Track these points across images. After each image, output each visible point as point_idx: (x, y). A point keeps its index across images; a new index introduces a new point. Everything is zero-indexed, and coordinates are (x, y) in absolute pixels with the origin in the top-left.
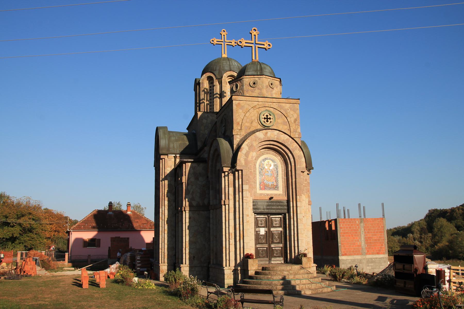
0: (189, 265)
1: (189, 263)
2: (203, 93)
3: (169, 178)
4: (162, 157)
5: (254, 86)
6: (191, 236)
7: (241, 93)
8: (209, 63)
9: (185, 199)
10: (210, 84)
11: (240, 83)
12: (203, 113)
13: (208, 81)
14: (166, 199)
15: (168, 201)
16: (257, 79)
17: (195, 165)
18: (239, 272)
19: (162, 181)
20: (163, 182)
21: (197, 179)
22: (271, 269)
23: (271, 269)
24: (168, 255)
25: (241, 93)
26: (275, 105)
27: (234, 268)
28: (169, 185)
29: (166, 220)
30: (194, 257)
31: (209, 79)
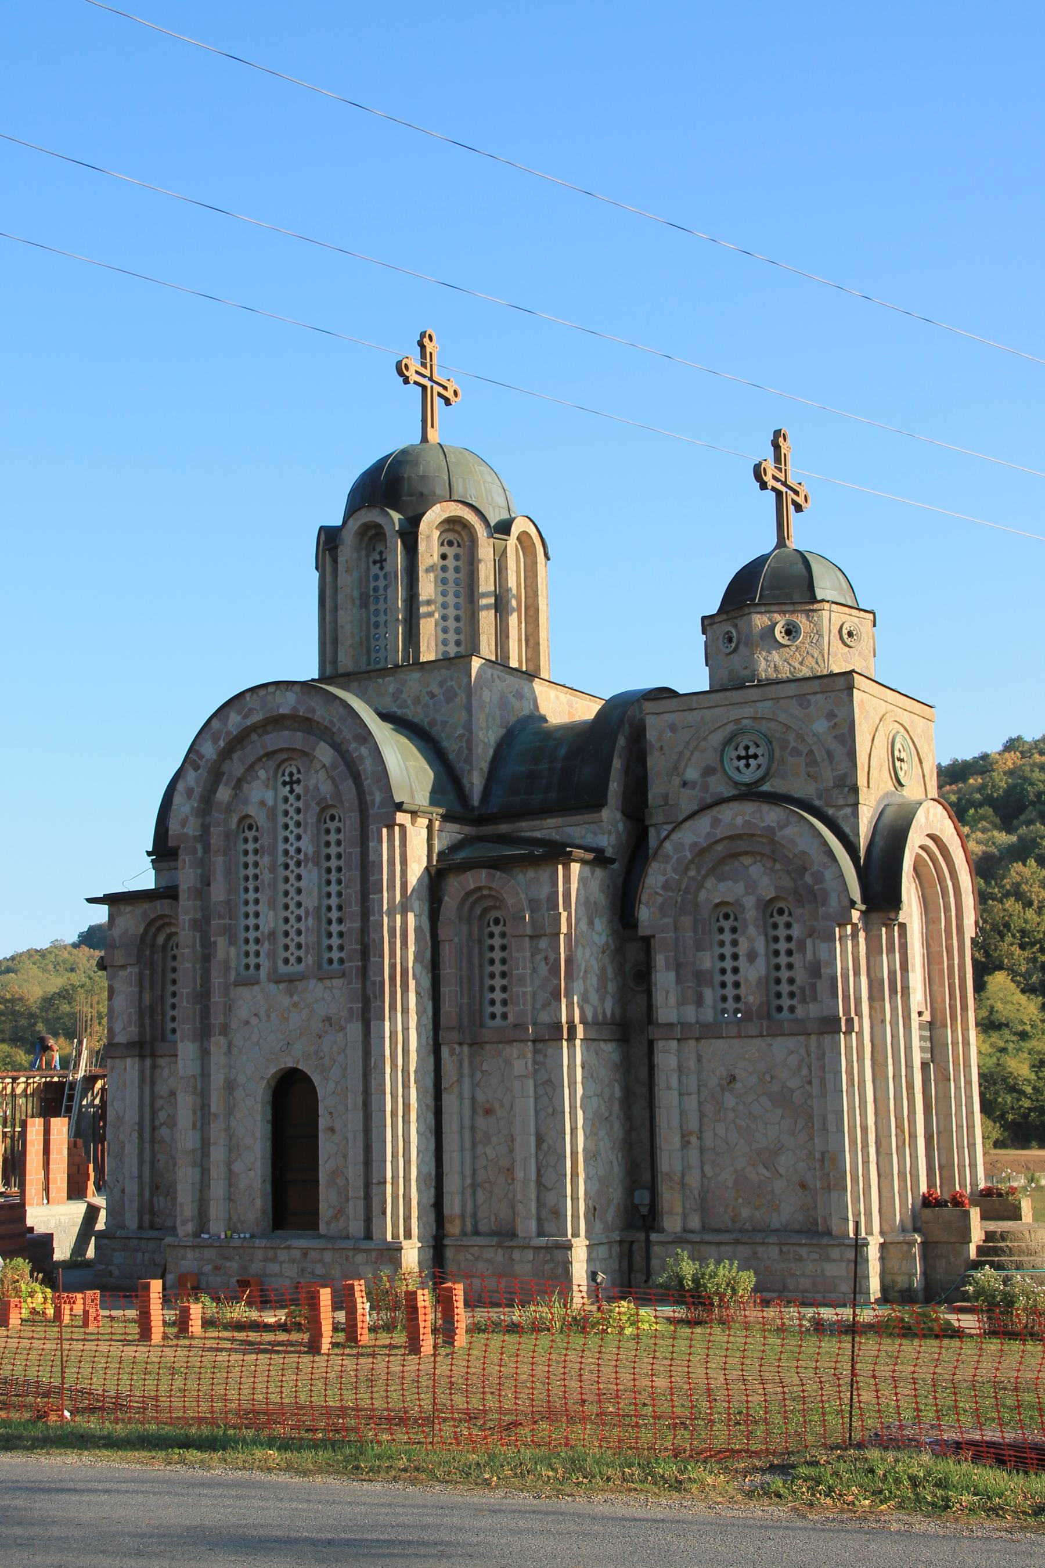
0: (587, 1238)
1: (587, 1231)
2: (432, 576)
3: (416, 904)
4: (401, 818)
5: (851, 644)
6: (588, 1133)
7: (813, 657)
8: (404, 452)
9: (569, 996)
10: (442, 544)
11: (804, 620)
12: (483, 665)
13: (438, 533)
14: (412, 984)
15: (418, 993)
16: (856, 620)
17: (587, 869)
18: (916, 1250)
19: (391, 915)
20: (398, 917)
21: (591, 923)
22: (1028, 1236)
23: (1028, 1236)
24: (418, 1204)
25: (813, 657)
26: (905, 718)
27: (882, 1241)
28: (418, 930)
29: (413, 1067)
30: (595, 1209)
31: (446, 526)
